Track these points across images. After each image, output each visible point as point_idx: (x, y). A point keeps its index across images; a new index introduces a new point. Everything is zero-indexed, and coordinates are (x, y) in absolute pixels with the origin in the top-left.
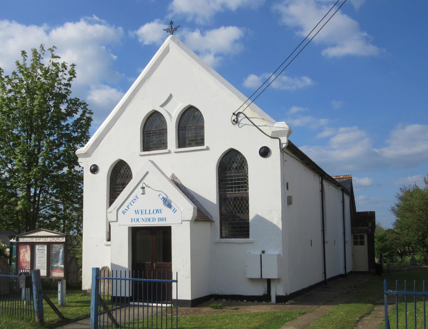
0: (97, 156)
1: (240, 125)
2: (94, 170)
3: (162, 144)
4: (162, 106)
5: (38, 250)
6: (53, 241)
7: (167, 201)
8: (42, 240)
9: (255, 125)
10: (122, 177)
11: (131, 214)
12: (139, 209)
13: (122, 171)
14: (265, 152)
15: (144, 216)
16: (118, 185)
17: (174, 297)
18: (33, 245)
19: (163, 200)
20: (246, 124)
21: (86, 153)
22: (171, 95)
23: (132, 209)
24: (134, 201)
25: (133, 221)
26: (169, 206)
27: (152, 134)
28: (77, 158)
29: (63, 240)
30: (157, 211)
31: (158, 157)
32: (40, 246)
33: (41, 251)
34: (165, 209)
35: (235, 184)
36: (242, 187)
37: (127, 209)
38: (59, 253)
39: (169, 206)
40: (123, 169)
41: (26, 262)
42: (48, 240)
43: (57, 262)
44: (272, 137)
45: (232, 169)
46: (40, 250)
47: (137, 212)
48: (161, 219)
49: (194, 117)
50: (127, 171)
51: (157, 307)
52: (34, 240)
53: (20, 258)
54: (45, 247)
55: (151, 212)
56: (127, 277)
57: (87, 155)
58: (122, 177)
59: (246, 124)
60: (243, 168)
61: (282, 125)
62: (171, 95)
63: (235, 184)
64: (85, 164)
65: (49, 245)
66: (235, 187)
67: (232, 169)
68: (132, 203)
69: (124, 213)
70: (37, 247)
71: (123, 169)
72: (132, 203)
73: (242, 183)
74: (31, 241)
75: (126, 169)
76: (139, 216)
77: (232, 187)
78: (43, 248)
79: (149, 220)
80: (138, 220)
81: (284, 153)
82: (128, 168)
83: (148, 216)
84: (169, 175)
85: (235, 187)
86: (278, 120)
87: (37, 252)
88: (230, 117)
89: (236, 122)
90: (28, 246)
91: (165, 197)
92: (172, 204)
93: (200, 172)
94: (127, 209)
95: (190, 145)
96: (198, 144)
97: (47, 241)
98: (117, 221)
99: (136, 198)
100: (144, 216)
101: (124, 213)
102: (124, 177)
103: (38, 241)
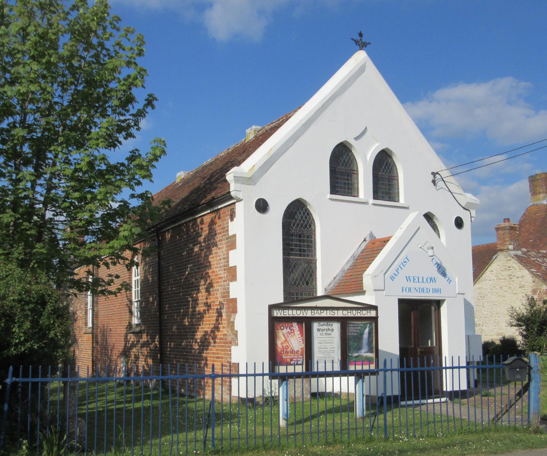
1: (438, 188)
4: (356, 139)
5: (319, 330)
6: (349, 315)
7: (441, 269)
8: (325, 314)
9: (450, 191)
10: (298, 225)
12: (411, 275)
13: (298, 216)
16: (292, 235)
17: (445, 389)
19: (436, 265)
20: (442, 188)
21: (250, 178)
22: (366, 128)
23: (403, 273)
24: (404, 264)
25: (404, 291)
26: (444, 274)
30: (431, 279)
32: (322, 323)
34: (439, 277)
37: (397, 274)
38: (362, 334)
39: (444, 274)
40: (300, 213)
41: (292, 352)
42: (340, 314)
43: (359, 349)
44: (464, 208)
46: (323, 330)
47: (408, 279)
48: (436, 291)
49: (387, 164)
50: (306, 217)
51: (434, 403)
52: (309, 314)
54: (336, 326)
55: (425, 280)
58: (298, 225)
59: (442, 188)
62: (366, 128)
68: (402, 266)
69: (392, 278)
70: (316, 326)
71: (300, 213)
72: (402, 266)
74: (301, 315)
75: (304, 214)
76: (411, 285)
78: (330, 327)
79: (423, 290)
80: (410, 290)
82: (308, 215)
83: (421, 285)
90: (295, 325)
91: (439, 262)
92: (447, 273)
94: (397, 274)
96: (390, 199)
97: (336, 315)
98: (384, 290)
99: (406, 260)
102: (302, 225)
103: (317, 315)
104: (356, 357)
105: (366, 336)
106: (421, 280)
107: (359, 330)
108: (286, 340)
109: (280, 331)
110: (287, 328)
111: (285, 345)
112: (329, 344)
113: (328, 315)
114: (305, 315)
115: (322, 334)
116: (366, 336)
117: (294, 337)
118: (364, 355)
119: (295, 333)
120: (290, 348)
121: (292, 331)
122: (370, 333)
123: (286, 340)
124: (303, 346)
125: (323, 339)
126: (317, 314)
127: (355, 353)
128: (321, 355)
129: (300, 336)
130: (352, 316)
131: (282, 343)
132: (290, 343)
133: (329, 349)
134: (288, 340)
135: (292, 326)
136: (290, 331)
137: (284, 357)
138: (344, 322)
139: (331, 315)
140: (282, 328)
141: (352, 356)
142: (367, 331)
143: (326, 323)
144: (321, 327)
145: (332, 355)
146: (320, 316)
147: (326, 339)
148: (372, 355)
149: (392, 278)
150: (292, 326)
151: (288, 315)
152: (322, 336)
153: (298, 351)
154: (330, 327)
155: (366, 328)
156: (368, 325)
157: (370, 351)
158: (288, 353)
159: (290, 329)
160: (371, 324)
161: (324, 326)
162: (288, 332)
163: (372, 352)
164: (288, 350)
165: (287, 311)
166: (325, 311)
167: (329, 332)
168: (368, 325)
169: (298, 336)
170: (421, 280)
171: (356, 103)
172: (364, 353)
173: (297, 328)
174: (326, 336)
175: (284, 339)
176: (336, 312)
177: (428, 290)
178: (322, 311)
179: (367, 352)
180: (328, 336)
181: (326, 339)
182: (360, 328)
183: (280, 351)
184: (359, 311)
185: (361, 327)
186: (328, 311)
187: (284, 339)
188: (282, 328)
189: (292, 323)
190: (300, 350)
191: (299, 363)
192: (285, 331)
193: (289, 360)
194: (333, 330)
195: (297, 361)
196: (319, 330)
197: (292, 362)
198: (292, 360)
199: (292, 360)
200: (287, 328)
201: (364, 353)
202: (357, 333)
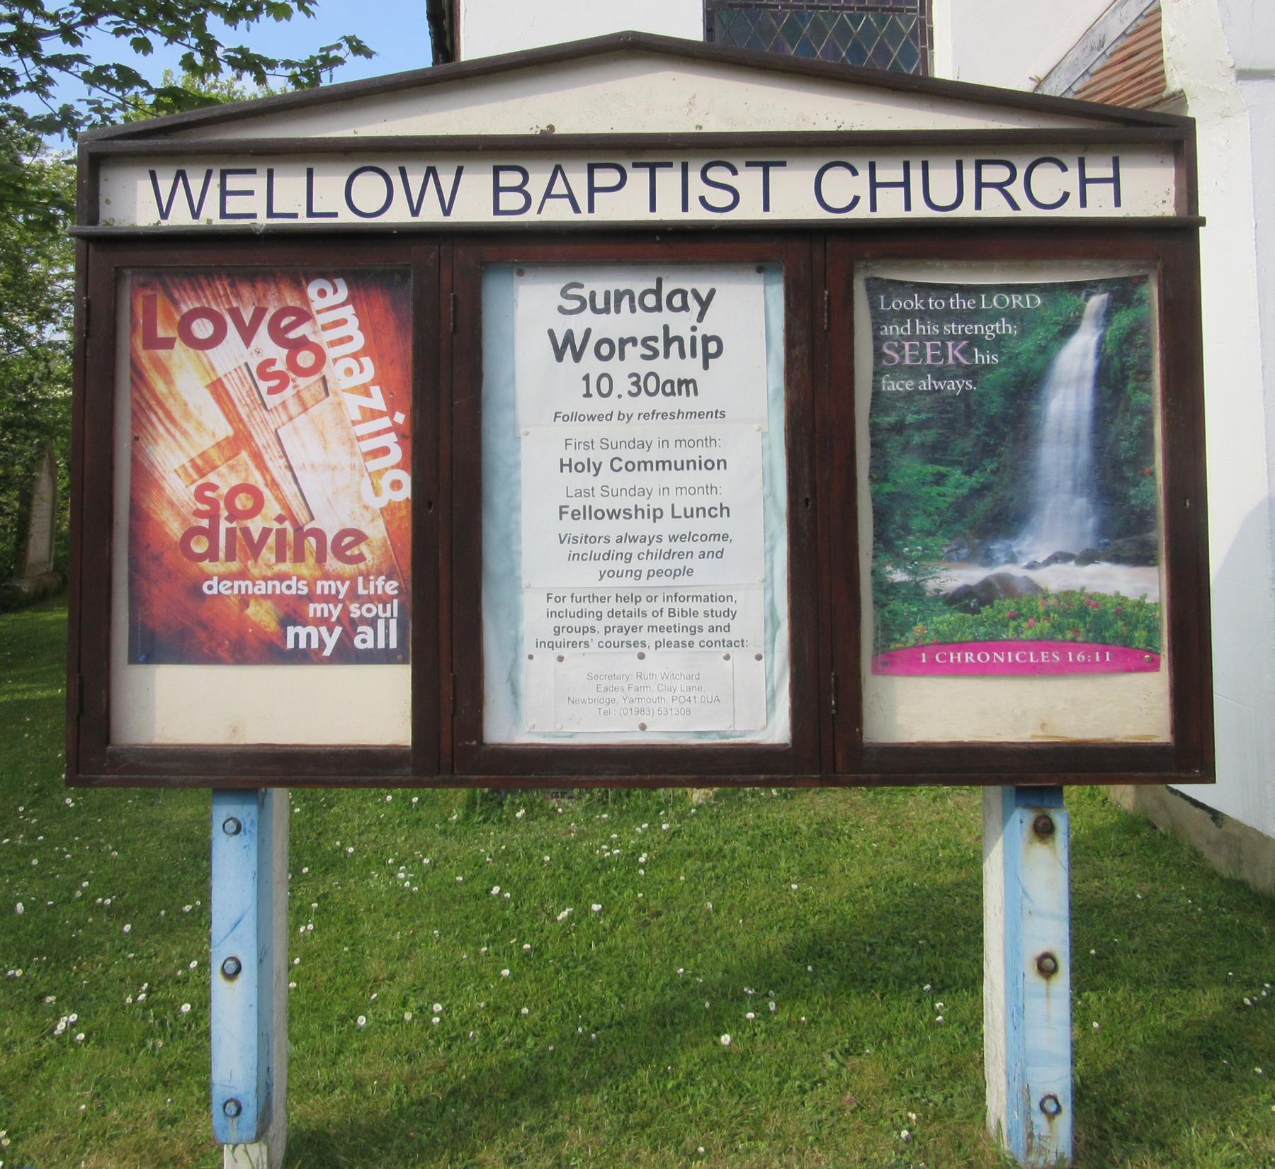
8: (627, 201)
32: (599, 284)
33: (634, 358)
38: (1027, 386)
41: (298, 539)
42: (793, 196)
43: (1000, 519)
46: (613, 348)
52: (474, 200)
53: (143, 474)
54: (748, 311)
70: (529, 311)
74: (398, 215)
78: (681, 324)
90: (332, 309)
97: (749, 211)
104: (961, 600)
105: (1068, 399)
107: (998, 343)
108: (240, 440)
109: (180, 355)
110: (247, 334)
111: (225, 480)
112: (671, 478)
113: (669, 211)
114: (431, 214)
115: (600, 387)
116: (1068, 399)
117: (322, 410)
118: (1057, 579)
119: (334, 372)
120: (272, 508)
121: (306, 359)
122: (1112, 379)
123: (240, 440)
124: (396, 486)
125: (615, 430)
126: (549, 200)
127: (951, 558)
128: (586, 577)
129: (377, 401)
130: (920, 210)
131: (202, 466)
132: (276, 466)
133: (666, 526)
134: (262, 439)
135: (304, 316)
136: (280, 354)
137: (212, 587)
138: (818, 268)
139: (697, 214)
140: (203, 329)
141: (915, 592)
142: (1078, 356)
143: (639, 283)
144: (578, 324)
145: (706, 575)
146: (584, 217)
147: (639, 429)
148: (1143, 585)
150: (304, 316)
151: (263, 221)
152: (597, 405)
153: (360, 537)
154: (681, 324)
155: (1068, 329)
156: (1096, 302)
157: (1120, 537)
158: (255, 549)
159: (278, 335)
160: (1122, 295)
161: (621, 307)
162: (264, 370)
163: (1143, 558)
164: (256, 526)
165: (257, 183)
166: (638, 179)
167: (672, 367)
168: (1096, 302)
169: (353, 404)
172: (1054, 558)
173: (353, 326)
174: (644, 403)
175: (224, 430)
176: (748, 180)
178: (606, 178)
179: (1087, 558)
180: (661, 403)
181: (639, 429)
182: (1004, 327)
183: (175, 529)
184: (994, 174)
185: (1014, 315)
186: (669, 180)
187: (224, 430)
188: (203, 329)
189: (298, 282)
190: (377, 531)
191: (365, 639)
192: (232, 356)
193: (262, 615)
194: (710, 350)
195: (350, 625)
196: (566, 347)
197: (296, 636)
198: (292, 612)
199: (292, 612)
200: (247, 334)
201: (1054, 558)
202: (972, 373)
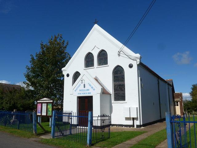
0: (68, 70)
2: (68, 75)
3: (92, 65)
8: (45, 101)
11: (78, 91)
14: (131, 66)
15: (83, 92)
18: (42, 103)
27: (89, 61)
28: (62, 71)
29: (52, 101)
31: (90, 70)
35: (120, 79)
36: (122, 80)
42: (47, 101)
45: (118, 74)
47: (80, 90)
48: (89, 93)
52: (43, 101)
54: (46, 104)
56: (76, 115)
57: (65, 70)
60: (123, 73)
61: (138, 55)
63: (120, 79)
64: (65, 73)
65: (47, 103)
66: (120, 81)
67: (118, 74)
70: (43, 104)
73: (122, 79)
76: (81, 92)
77: (118, 81)
79: (84, 93)
81: (139, 67)
83: (84, 92)
84: (94, 77)
85: (120, 81)
86: (136, 53)
87: (43, 106)
88: (117, 53)
89: (119, 55)
93: (105, 75)
95: (103, 65)
96: (105, 64)
100: (83, 92)
101: (75, 91)
106: (84, 90)
149: (75, 91)
170: (84, 90)
171: (98, 38)
177: (86, 93)
